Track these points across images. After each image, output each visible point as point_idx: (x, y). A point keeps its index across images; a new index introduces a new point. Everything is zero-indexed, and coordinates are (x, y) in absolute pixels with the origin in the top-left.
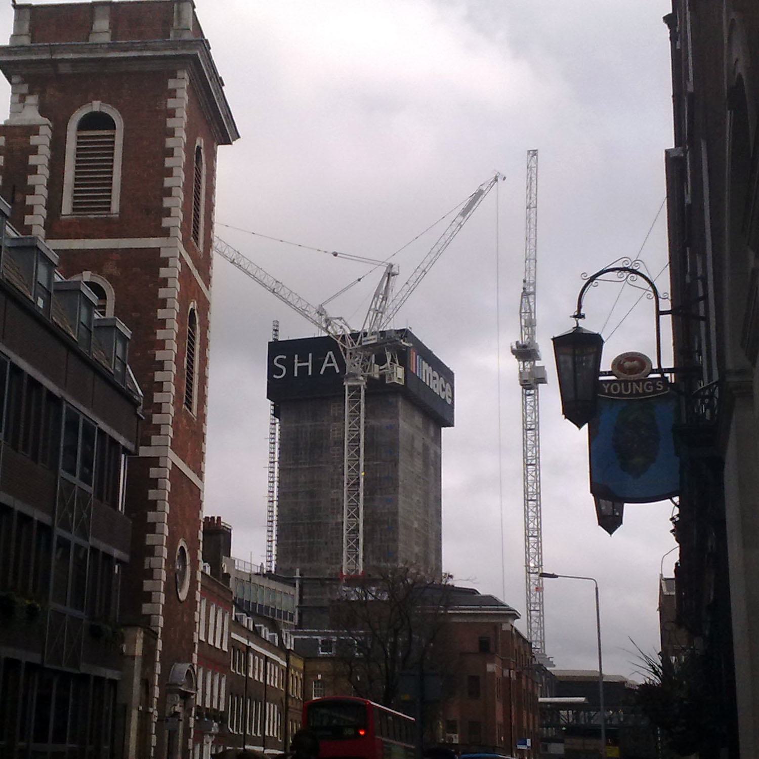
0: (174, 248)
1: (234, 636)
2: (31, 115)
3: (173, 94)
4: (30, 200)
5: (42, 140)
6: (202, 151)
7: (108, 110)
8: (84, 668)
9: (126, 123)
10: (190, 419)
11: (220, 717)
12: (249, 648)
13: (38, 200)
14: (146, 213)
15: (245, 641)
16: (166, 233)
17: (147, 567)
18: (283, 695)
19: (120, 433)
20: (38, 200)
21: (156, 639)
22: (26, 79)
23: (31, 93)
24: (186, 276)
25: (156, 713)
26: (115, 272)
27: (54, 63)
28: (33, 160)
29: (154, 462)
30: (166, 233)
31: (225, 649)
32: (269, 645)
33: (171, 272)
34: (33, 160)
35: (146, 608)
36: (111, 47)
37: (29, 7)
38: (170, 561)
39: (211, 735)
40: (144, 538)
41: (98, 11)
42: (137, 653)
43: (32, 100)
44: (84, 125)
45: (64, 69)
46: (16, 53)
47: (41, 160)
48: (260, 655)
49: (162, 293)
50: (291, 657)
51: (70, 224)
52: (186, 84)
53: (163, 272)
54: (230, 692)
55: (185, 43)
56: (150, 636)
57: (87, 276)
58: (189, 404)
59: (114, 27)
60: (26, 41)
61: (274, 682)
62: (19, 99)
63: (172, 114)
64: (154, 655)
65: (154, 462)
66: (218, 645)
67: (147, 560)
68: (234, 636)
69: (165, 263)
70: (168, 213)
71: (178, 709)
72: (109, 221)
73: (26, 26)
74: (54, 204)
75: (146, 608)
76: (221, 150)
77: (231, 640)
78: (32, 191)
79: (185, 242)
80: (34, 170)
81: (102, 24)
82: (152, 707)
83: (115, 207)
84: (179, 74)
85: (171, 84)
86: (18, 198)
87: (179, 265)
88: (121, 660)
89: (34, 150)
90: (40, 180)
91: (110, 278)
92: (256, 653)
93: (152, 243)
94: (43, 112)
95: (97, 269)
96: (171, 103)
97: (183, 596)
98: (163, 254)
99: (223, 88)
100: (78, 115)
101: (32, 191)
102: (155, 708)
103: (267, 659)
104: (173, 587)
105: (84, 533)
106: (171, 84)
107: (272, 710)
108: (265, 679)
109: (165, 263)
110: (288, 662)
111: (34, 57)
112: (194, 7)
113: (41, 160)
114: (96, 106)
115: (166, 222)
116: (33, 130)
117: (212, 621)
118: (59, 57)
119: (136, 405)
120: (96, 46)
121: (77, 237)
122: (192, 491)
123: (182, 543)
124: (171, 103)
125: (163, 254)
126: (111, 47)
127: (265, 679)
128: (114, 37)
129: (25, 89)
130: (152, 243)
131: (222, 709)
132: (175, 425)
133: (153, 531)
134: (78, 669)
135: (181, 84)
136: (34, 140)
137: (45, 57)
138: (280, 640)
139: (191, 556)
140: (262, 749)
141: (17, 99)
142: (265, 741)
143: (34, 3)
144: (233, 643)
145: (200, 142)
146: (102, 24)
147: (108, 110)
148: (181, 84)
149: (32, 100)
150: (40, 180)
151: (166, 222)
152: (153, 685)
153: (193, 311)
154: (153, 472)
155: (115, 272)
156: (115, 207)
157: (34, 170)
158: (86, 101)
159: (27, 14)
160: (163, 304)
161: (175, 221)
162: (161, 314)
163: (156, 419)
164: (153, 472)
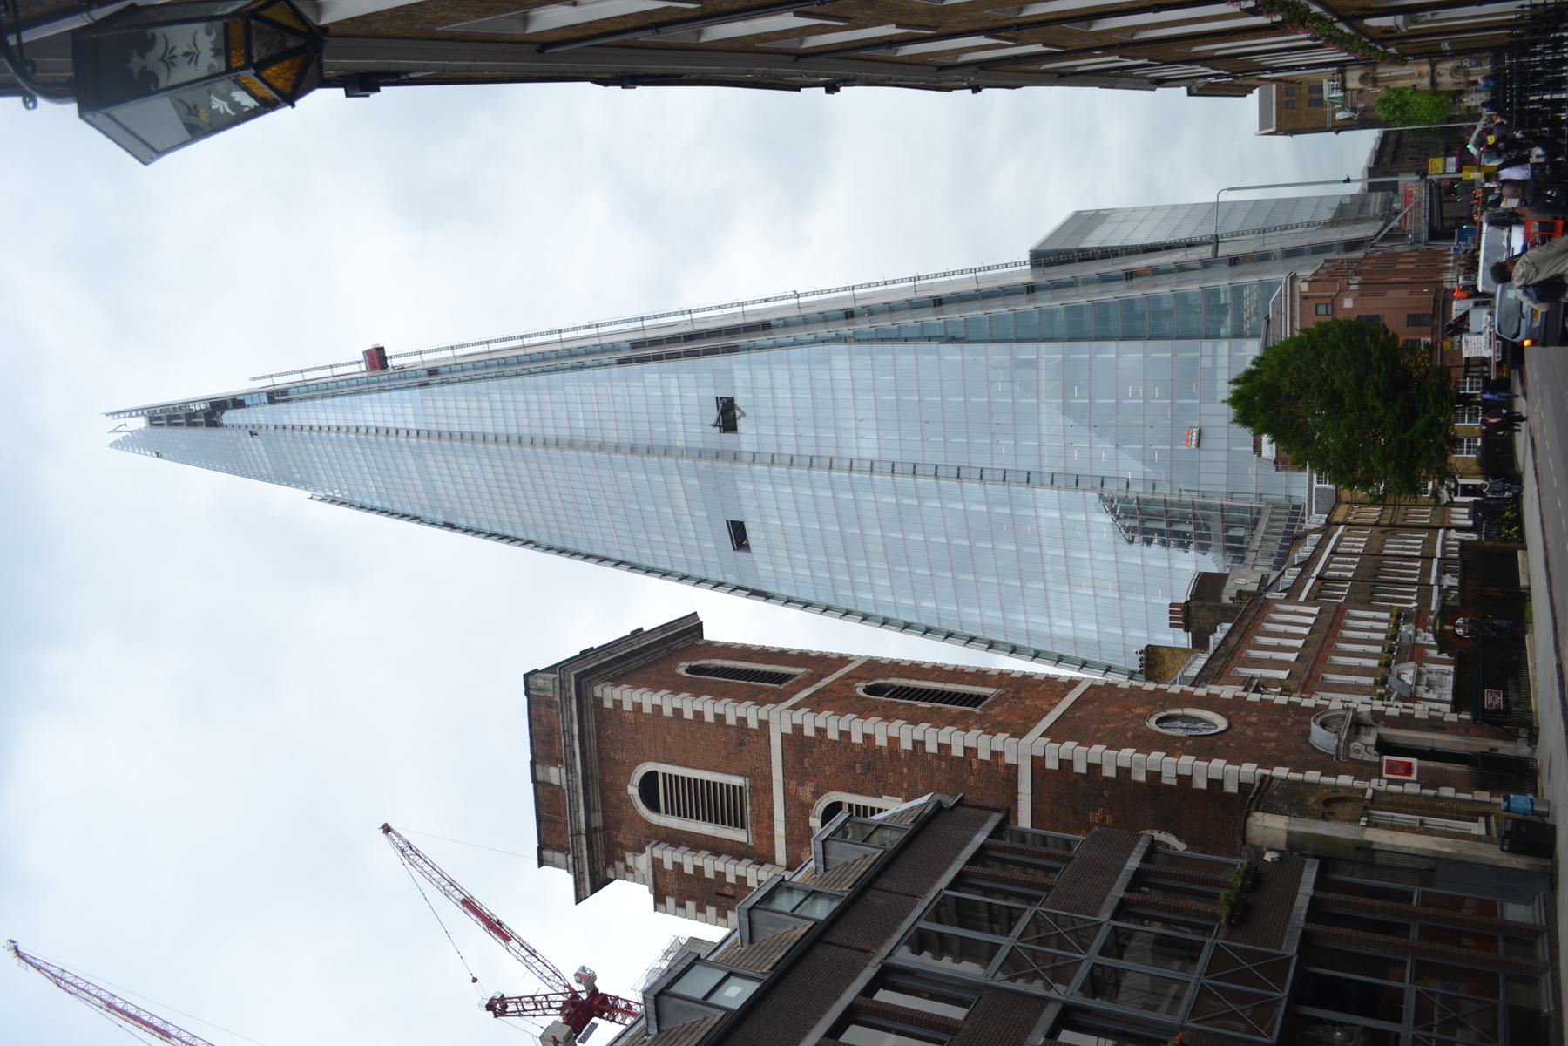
1: (1302, 598)
2: (643, 862)
3: (618, 704)
4: (731, 879)
5: (669, 857)
6: (694, 664)
7: (637, 777)
8: (1290, 948)
9: (649, 760)
10: (999, 700)
11: (1399, 617)
12: (1319, 578)
13: (732, 870)
14: (744, 744)
15: (1311, 582)
17: (1174, 782)
18: (1376, 530)
19: (968, 840)
20: (732, 870)
21: (1272, 778)
22: (610, 862)
23: (623, 860)
24: (816, 704)
25: (1374, 782)
28: (688, 870)
29: (1037, 762)
30: (764, 725)
31: (1315, 610)
32: (1320, 547)
33: (810, 723)
34: (688, 870)
35: (1231, 788)
36: (570, 768)
37: (540, 850)
38: (1171, 746)
39: (1416, 634)
40: (1137, 783)
42: (1284, 827)
44: (653, 806)
45: (597, 820)
46: (582, 873)
47: (689, 861)
48: (1329, 560)
49: (833, 735)
50: (1338, 518)
51: (758, 835)
52: (607, 690)
53: (809, 732)
54: (1368, 604)
56: (1260, 796)
57: (815, 822)
58: (975, 700)
59: (556, 762)
60: (570, 859)
61: (1359, 543)
62: (629, 872)
63: (638, 707)
64: (1295, 782)
65: (1037, 762)
66: (1311, 620)
67: (1165, 781)
68: (1302, 598)
69: (798, 729)
71: (1371, 740)
72: (753, 789)
73: (559, 856)
74: (738, 852)
75: (1231, 788)
76: (708, 635)
77: (1307, 602)
78: (720, 875)
79: (780, 698)
80: (699, 870)
81: (555, 775)
82: (1364, 791)
84: (598, 693)
86: (730, 892)
87: (804, 710)
88: (1296, 848)
89: (679, 866)
90: (711, 866)
91: (817, 795)
92: (1326, 567)
93: (776, 742)
94: (642, 851)
95: (806, 809)
97: (1221, 723)
98: (789, 731)
99: (646, 629)
100: (643, 810)
101: (720, 875)
102: (1366, 784)
103: (1333, 552)
104: (1205, 747)
105: (1082, 938)
106: (608, 704)
107: (1393, 545)
108: (1355, 555)
109: (798, 729)
110: (1338, 524)
111: (585, 853)
112: (536, 671)
113: (689, 861)
114: (633, 790)
115: (753, 724)
116: (657, 864)
117: (1282, 628)
118: (583, 827)
119: (939, 808)
121: (771, 827)
122: (1091, 701)
123: (1152, 723)
124: (627, 706)
125: (789, 731)
126: (570, 768)
127: (1355, 555)
129: (620, 865)
130: (776, 742)
131: (1387, 615)
132: (992, 731)
133: (1128, 771)
134: (1290, 959)
135: (609, 694)
136: (668, 865)
137: (584, 842)
138: (1315, 531)
139: (1171, 707)
140: (1435, 561)
141: (629, 875)
142: (1427, 557)
143: (537, 844)
144: (1312, 600)
145: (681, 669)
146: (555, 775)
148: (609, 694)
149: (630, 860)
150: (711, 866)
151: (753, 724)
152: (1335, 788)
153: (868, 690)
154: (1052, 764)
156: (738, 781)
157: (699, 870)
158: (629, 800)
159: (547, 854)
160: (845, 735)
161: (752, 714)
162: (857, 738)
163: (984, 755)
164: (1052, 764)
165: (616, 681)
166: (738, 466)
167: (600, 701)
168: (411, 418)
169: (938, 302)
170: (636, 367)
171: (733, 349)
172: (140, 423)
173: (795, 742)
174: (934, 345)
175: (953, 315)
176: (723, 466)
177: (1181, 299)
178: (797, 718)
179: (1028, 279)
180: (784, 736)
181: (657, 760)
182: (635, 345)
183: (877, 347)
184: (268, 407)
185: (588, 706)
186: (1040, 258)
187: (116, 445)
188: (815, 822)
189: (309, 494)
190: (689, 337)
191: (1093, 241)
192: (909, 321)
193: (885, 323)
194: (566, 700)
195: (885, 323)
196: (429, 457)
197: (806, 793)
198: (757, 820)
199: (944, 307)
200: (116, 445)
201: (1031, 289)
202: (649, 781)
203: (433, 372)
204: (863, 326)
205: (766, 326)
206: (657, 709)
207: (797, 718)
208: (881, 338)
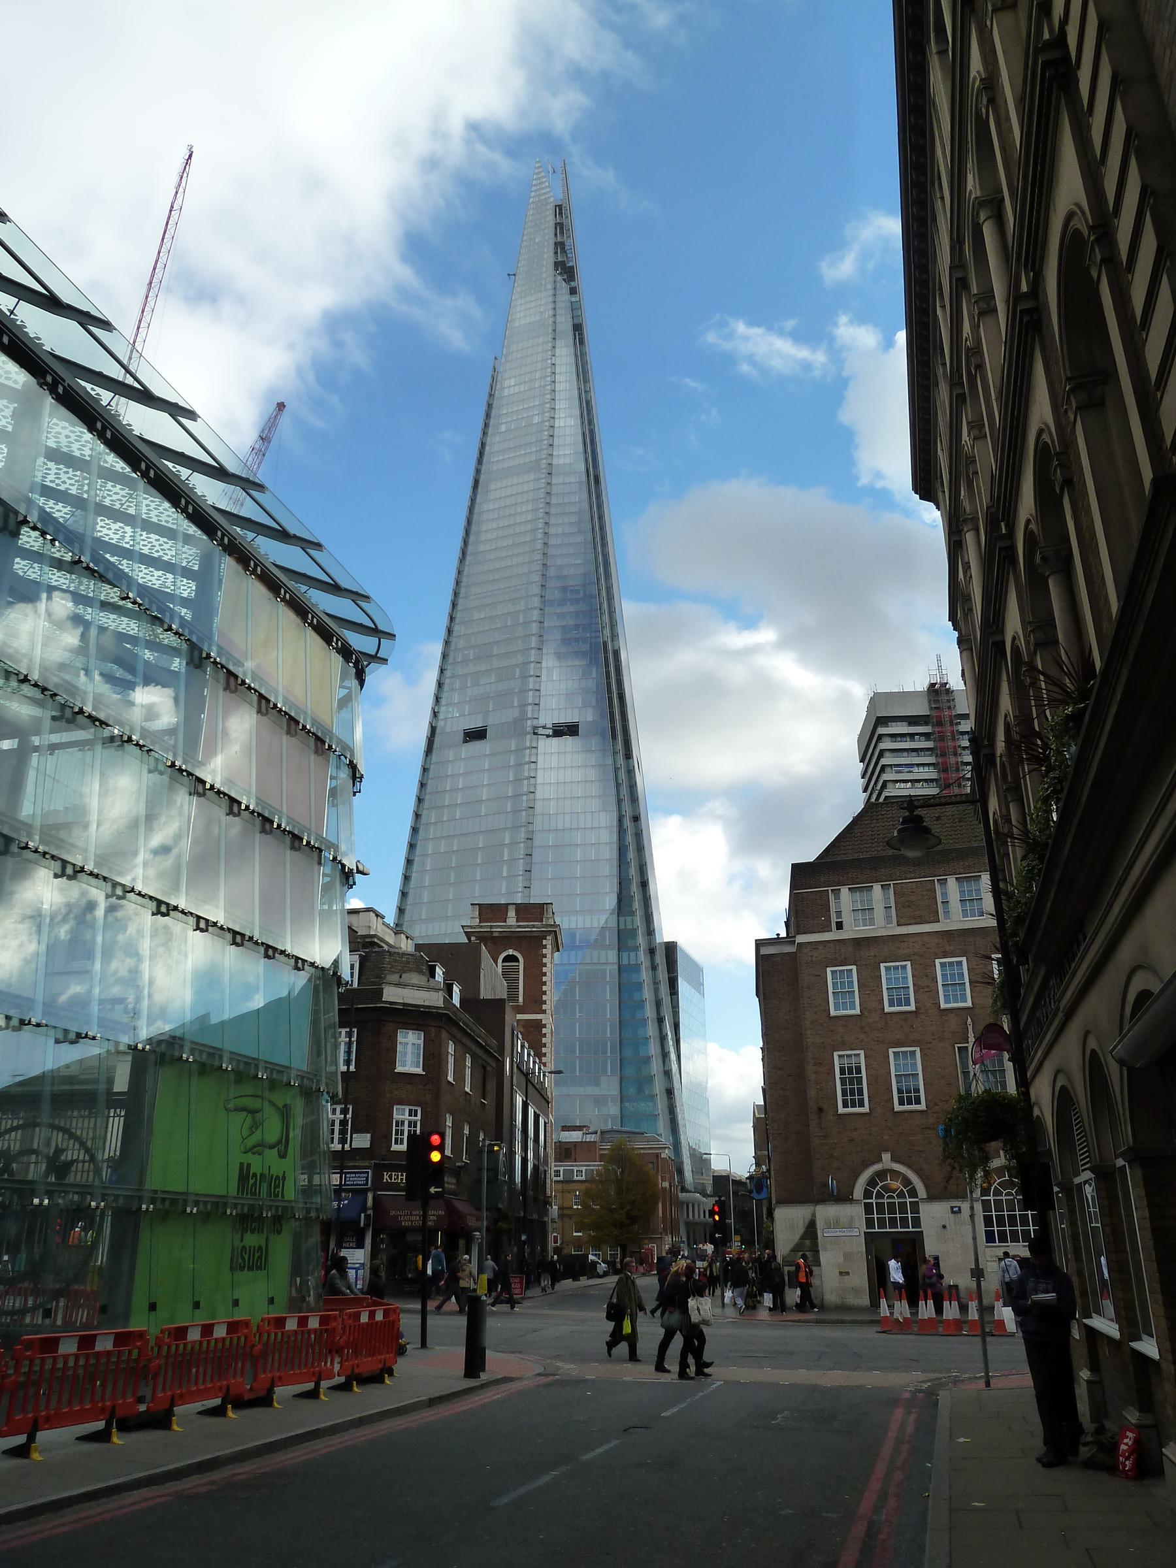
7: (516, 954)
16: (544, 1012)
30: (544, 1012)
41: (510, 907)
44: (506, 959)
53: (544, 1031)
69: (545, 1026)
81: (512, 913)
83: (521, 999)
85: (544, 942)
93: (538, 1017)
106: (544, 942)
114: (511, 952)
115: (544, 1007)
120: (510, 926)
124: (544, 951)
130: (538, 1017)
146: (512, 913)
147: (516, 954)
148: (548, 942)
151: (544, 1007)
156: (521, 999)
168: (561, 462)
169: (644, 885)
171: (614, 736)
173: (539, 1025)
175: (635, 888)
177: (648, 1059)
179: (658, 941)
183: (615, 846)
184: (552, 242)
186: (671, 949)
190: (622, 697)
191: (683, 986)
192: (633, 872)
193: (631, 855)
195: (630, 838)
196: (532, 477)
201: (652, 951)
202: (515, 959)
204: (628, 823)
205: (628, 755)
208: (622, 850)
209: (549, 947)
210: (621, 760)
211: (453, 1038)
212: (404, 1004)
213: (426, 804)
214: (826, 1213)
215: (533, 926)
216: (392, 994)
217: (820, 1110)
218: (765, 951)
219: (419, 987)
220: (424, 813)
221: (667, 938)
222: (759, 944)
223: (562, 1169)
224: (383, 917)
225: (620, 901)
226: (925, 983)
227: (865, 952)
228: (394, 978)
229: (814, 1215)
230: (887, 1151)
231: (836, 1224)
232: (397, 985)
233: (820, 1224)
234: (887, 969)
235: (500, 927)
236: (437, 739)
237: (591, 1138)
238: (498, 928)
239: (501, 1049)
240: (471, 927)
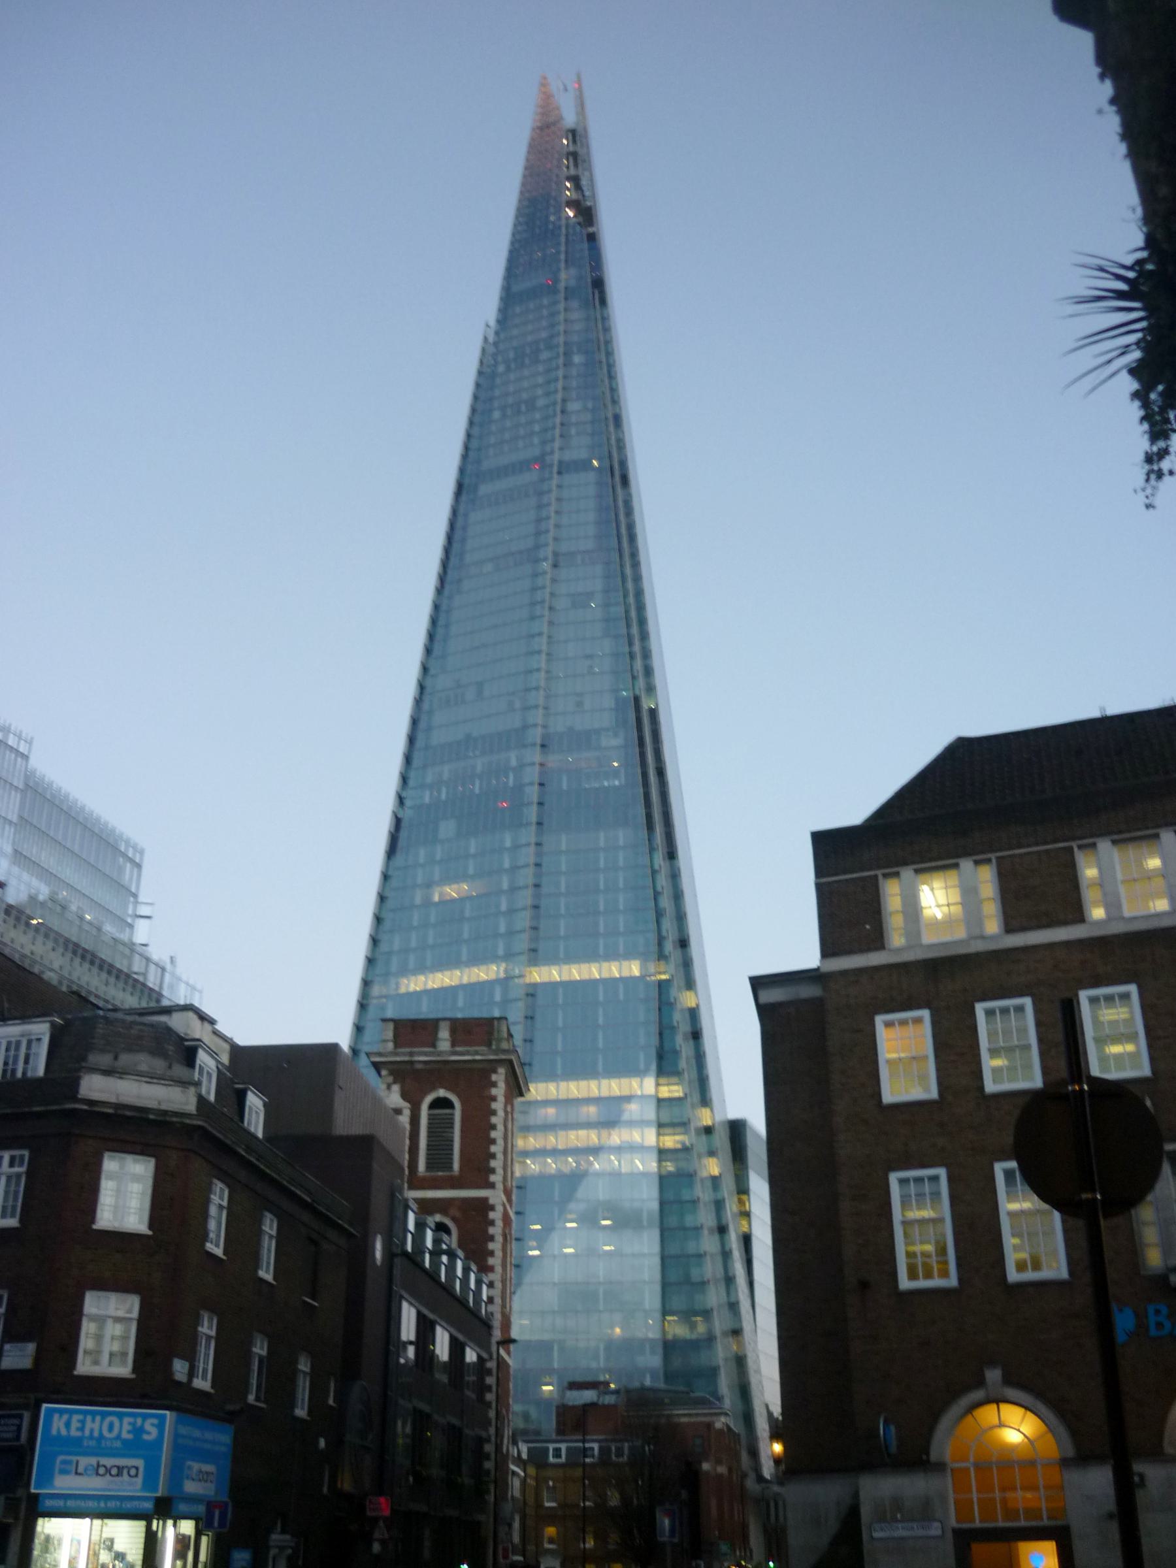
0: (496, 1197)
3: (494, 1085)
14: (478, 1169)
16: (492, 1186)
22: (391, 1073)
23: (395, 1082)
26: (458, 1214)
27: (412, 1063)
30: (492, 1186)
43: (396, 1088)
45: (419, 1066)
51: (424, 1179)
53: (492, 1215)
55: (505, 1051)
63: (494, 1099)
69: (492, 1208)
70: (493, 1171)
72: (452, 1178)
81: (444, 1034)
83: (456, 1166)
91: (454, 1219)
94: (404, 1096)
95: (444, 1212)
96: (494, 1091)
106: (494, 1077)
109: (492, 1208)
114: (442, 1093)
115: (492, 1178)
116: (398, 1111)
120: (440, 1053)
124: (494, 1091)
128: (453, 1045)
146: (444, 1034)
148: (500, 1077)
151: (492, 1178)
155: (458, 1214)
156: (456, 1166)
158: (433, 1088)
159: (391, 1026)
165: (507, 1082)
166: (534, 828)
167: (495, 1072)
169: (696, 1035)
170: (632, 716)
172: (569, 118)
173: (484, 1206)
174: (655, 1040)
176: (532, 814)
178: (500, 1209)
180: (486, 1200)
181: (463, 1111)
182: (653, 713)
185: (492, 1066)
187: (544, 83)
188: (438, 1218)
189: (492, 323)
190: (661, 772)
194: (496, 1052)
197: (454, 1212)
198: (435, 1179)
199: (691, 1042)
200: (544, 83)
203: (625, 481)
205: (672, 855)
206: (494, 1113)
207: (500, 1209)
209: (502, 1085)
210: (659, 859)
211: (225, 1177)
212: (118, 1106)
213: (387, 925)
214: (876, 1489)
215: (477, 1053)
216: (96, 1087)
217: (864, 1285)
218: (772, 996)
219: (152, 1077)
220: (384, 938)
221: (733, 1115)
222: (758, 983)
223: (563, 1447)
224: (212, 1022)
225: (660, 1057)
226: (1064, 1036)
227: (947, 984)
228: (105, 1060)
229: (856, 1495)
230: (992, 1363)
231: (893, 1511)
232: (108, 1072)
233: (865, 1511)
234: (990, 1013)
235: (426, 1054)
236: (403, 834)
237: (609, 1400)
238: (422, 1056)
239: (362, 1217)
240: (380, 1054)
